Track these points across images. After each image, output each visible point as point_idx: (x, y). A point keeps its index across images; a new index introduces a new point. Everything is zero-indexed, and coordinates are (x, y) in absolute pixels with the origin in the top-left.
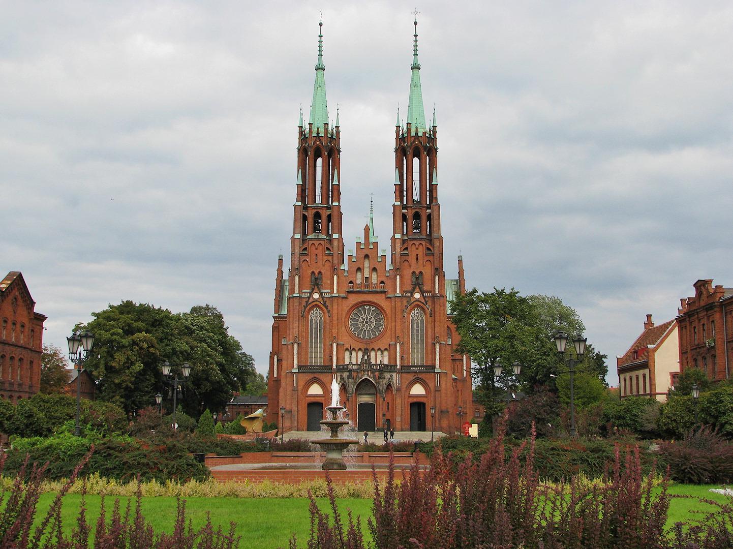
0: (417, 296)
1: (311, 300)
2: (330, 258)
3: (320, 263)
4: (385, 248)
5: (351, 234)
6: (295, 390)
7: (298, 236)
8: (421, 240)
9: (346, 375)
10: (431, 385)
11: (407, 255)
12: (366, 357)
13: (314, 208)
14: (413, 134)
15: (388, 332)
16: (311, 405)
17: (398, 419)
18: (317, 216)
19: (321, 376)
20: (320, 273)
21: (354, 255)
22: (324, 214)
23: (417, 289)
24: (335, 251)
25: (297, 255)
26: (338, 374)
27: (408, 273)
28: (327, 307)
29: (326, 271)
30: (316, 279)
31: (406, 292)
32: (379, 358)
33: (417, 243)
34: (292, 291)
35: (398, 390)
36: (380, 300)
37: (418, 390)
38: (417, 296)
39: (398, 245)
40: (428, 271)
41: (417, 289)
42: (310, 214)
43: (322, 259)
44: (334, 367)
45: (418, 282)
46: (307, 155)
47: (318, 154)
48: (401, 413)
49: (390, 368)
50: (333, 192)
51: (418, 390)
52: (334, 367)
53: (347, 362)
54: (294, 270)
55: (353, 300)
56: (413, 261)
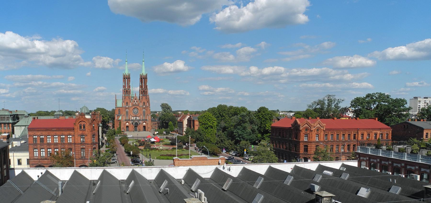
5: (132, 94)
22: (128, 91)
29: (129, 102)
32: (138, 118)
36: (138, 107)
37: (144, 124)
40: (146, 102)
43: (128, 99)
45: (144, 103)
48: (142, 128)
49: (140, 120)
51: (144, 124)
55: (134, 107)
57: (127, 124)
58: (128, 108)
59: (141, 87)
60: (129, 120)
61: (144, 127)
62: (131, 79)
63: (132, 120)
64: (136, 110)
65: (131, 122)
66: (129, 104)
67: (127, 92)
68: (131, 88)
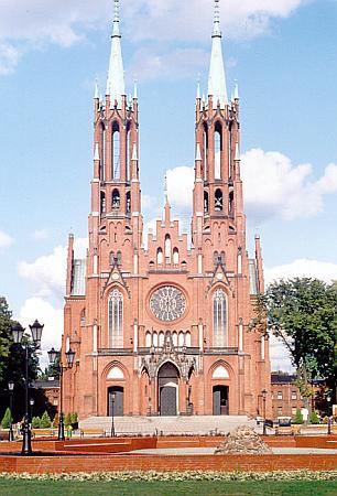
0: (220, 276)
1: (110, 281)
2: (129, 237)
3: (120, 242)
4: (184, 227)
6: (95, 374)
7: (97, 214)
8: (224, 218)
9: (148, 357)
10: (235, 368)
11: (208, 234)
12: (168, 340)
13: (112, 185)
14: (215, 107)
15: (190, 314)
16: (112, 390)
17: (201, 403)
18: (116, 193)
19: (122, 360)
20: (119, 252)
21: (155, 234)
22: (123, 191)
23: (220, 270)
24: (134, 230)
25: (95, 234)
26: (140, 357)
27: (209, 253)
28: (126, 288)
29: (126, 252)
30: (116, 259)
31: (209, 272)
33: (219, 221)
34: (90, 269)
35: (201, 373)
37: (221, 373)
38: (220, 276)
39: (200, 223)
40: (231, 251)
41: (220, 270)
42: (108, 191)
43: (121, 237)
44: (135, 350)
45: (220, 262)
46: (104, 129)
47: (115, 127)
48: (204, 397)
49: (193, 351)
50: (132, 167)
52: (135, 350)
53: (148, 345)
54: (95, 250)
55: (155, 280)
56: (215, 242)
57: (116, 373)
58: (124, 286)
59: (203, 168)
60: (128, 352)
61: (222, 391)
62: (141, 131)
63: (143, 352)
64: (168, 295)
65: (137, 363)
66: (125, 261)
67: (115, 197)
68: (144, 179)
